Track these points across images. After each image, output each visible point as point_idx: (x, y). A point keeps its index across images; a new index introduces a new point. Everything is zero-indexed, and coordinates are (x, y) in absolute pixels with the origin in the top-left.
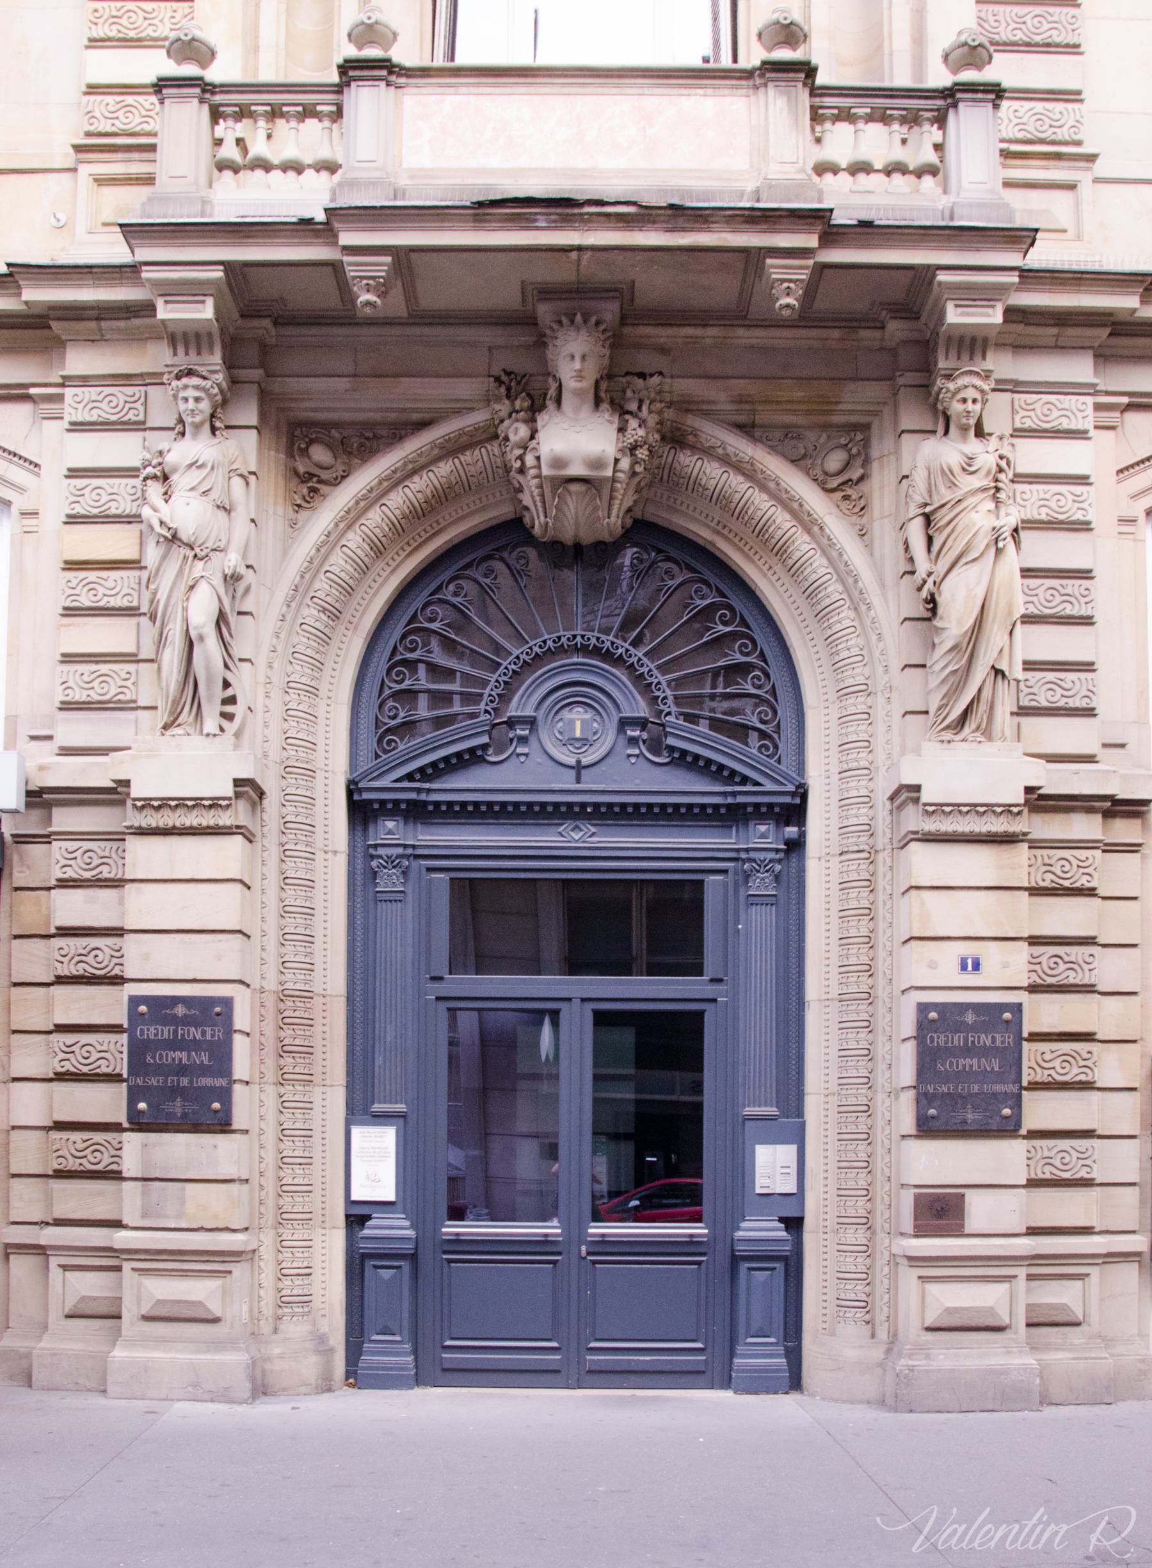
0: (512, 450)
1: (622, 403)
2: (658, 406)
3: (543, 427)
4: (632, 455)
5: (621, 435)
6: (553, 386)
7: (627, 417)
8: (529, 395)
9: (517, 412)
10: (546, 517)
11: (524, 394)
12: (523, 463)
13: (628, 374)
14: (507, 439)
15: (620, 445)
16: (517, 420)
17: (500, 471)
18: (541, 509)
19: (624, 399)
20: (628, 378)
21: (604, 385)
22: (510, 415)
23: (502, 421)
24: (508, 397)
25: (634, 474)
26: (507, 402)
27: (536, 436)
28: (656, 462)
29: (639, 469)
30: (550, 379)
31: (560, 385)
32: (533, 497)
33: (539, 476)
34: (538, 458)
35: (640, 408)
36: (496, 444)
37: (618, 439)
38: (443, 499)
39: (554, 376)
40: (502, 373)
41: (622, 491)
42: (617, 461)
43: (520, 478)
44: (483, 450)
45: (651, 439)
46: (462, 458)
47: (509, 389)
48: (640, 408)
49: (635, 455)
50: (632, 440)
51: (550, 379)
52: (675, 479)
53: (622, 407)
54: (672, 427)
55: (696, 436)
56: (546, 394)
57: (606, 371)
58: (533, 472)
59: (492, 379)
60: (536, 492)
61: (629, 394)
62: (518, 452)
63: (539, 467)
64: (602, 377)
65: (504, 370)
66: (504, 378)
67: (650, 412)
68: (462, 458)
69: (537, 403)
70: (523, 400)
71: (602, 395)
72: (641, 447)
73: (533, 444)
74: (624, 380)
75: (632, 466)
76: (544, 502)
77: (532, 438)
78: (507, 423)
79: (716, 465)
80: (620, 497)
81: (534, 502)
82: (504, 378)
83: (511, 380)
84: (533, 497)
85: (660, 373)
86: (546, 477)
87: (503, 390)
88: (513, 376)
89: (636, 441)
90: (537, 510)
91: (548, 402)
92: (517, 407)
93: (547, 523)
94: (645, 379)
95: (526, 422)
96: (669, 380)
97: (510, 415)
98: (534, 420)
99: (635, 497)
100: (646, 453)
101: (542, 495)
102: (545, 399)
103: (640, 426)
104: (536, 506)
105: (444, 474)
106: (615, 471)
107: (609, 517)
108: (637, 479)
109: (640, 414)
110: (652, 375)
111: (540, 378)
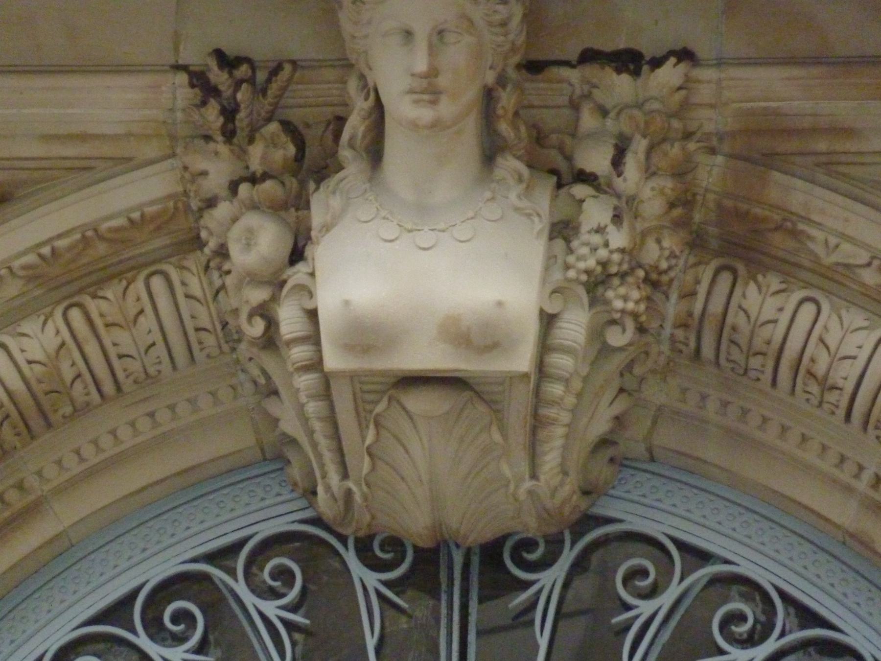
0: (239, 287)
1: (568, 141)
2: (675, 151)
3: (327, 228)
4: (593, 302)
5: (560, 243)
6: (361, 105)
7: (580, 190)
8: (288, 127)
9: (253, 180)
10: (345, 476)
11: (273, 127)
12: (271, 324)
13: (589, 57)
14: (222, 252)
15: (557, 276)
16: (254, 206)
17: (209, 340)
18: (328, 457)
19: (573, 135)
20: (591, 71)
21: (507, 100)
22: (233, 187)
23: (211, 203)
24: (229, 134)
25: (605, 350)
26: (223, 149)
27: (308, 252)
28: (672, 308)
29: (616, 338)
30: (353, 85)
31: (379, 106)
32: (305, 420)
33: (316, 365)
34: (313, 314)
35: (617, 162)
36: (194, 261)
37: (550, 259)
38: (36, 422)
39: (362, 77)
40: (213, 64)
41: (570, 400)
42: (548, 320)
43: (268, 361)
44: (157, 283)
45: (652, 253)
46: (93, 306)
47: (229, 113)
48: (617, 162)
49: (607, 302)
50: (591, 263)
51: (353, 85)
52: (736, 354)
53: (569, 158)
54: (719, 206)
55: (795, 234)
56: (341, 120)
57: (516, 59)
58: (300, 353)
59: (182, 78)
60: (313, 408)
61: (588, 120)
62: (258, 295)
63: (314, 339)
64: (502, 81)
65: (219, 55)
66: (219, 77)
67: (649, 172)
68: (93, 306)
69: (312, 151)
70: (273, 143)
71: (504, 127)
72: (623, 276)
73: (298, 274)
74: (573, 75)
75: (596, 334)
76: (336, 435)
77: (297, 255)
78: (223, 210)
79: (856, 318)
80: (565, 417)
81: (310, 433)
82: (219, 77)
83: (238, 84)
84: (305, 420)
85: (685, 55)
86: (340, 374)
87: (212, 115)
88: (243, 71)
89: (604, 264)
90: (319, 456)
91: (345, 153)
92: (256, 166)
93: (349, 493)
94: (636, 73)
95: (277, 208)
96: (706, 74)
97: (233, 187)
98: (302, 203)
99: (619, 407)
100: (635, 294)
101: (332, 420)
102: (337, 136)
103: (617, 218)
104: (315, 445)
105: (39, 356)
106: (545, 347)
107: (534, 476)
108: (617, 361)
109: (618, 183)
110: (657, 63)
111: (330, 74)
